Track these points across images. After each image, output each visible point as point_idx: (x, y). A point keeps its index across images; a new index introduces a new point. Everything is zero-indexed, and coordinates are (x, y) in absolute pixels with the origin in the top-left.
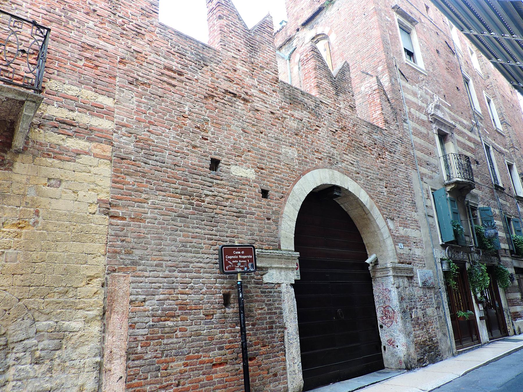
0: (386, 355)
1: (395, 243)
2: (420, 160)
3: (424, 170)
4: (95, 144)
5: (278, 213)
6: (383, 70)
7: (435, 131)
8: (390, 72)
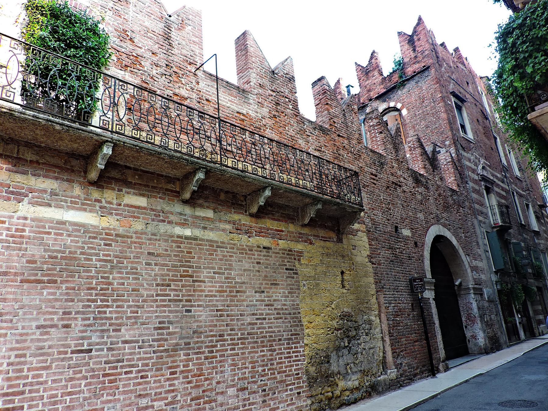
0: (470, 345)
1: (472, 271)
2: (478, 210)
3: (480, 218)
4: (360, 225)
5: (422, 256)
6: (449, 145)
7: (483, 187)
8: (456, 146)
